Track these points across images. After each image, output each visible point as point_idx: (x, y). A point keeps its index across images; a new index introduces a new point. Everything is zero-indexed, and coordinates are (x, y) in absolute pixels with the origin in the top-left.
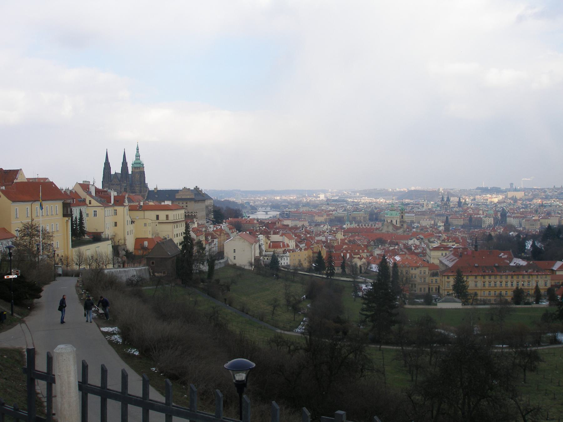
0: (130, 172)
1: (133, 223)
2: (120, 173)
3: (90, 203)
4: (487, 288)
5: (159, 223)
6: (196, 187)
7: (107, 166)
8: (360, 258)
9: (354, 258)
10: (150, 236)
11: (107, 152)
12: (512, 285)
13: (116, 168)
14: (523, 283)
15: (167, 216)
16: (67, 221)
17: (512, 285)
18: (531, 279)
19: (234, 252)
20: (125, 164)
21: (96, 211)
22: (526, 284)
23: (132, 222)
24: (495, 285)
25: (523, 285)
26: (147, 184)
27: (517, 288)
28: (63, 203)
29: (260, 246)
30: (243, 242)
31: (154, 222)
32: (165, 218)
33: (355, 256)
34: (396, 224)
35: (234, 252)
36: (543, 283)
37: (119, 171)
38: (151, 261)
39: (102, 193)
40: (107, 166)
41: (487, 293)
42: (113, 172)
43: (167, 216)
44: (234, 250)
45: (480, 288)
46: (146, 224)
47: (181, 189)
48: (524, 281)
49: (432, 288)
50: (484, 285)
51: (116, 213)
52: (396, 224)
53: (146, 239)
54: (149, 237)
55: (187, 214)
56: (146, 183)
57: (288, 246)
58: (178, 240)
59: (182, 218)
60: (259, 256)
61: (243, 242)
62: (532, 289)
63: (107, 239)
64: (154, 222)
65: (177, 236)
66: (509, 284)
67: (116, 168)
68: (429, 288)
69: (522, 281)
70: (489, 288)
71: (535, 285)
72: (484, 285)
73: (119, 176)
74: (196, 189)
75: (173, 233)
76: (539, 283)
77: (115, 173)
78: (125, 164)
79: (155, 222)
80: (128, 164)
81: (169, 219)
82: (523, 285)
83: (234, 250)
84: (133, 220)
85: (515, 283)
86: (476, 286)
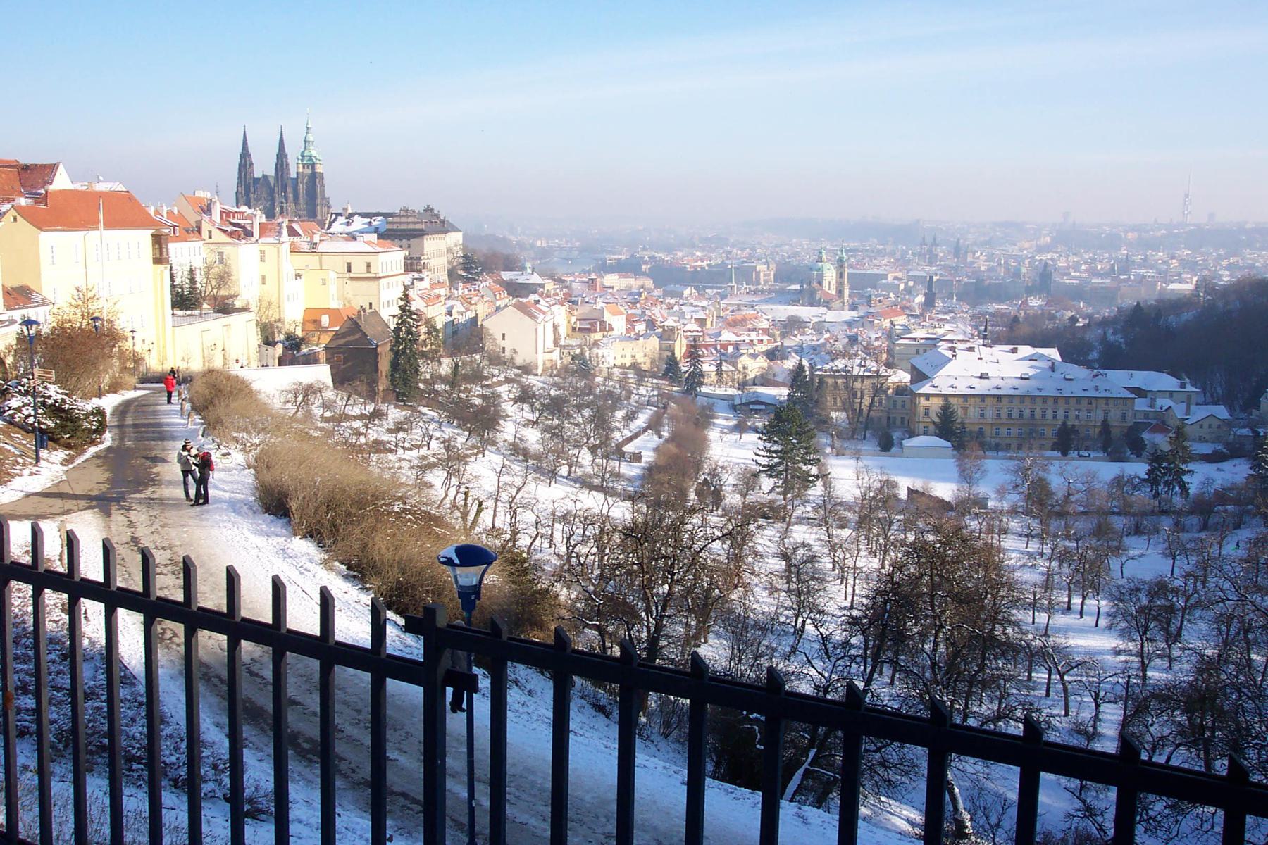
2: (273, 175)
3: (210, 237)
4: (1005, 421)
5: (352, 279)
6: (428, 206)
8: (754, 356)
9: (742, 354)
10: (334, 304)
12: (1055, 417)
13: (264, 166)
14: (1077, 413)
15: (369, 265)
16: (162, 271)
17: (1055, 417)
18: (1094, 405)
19: (504, 339)
20: (281, 155)
22: (1084, 415)
23: (298, 276)
24: (1021, 416)
25: (1077, 417)
27: (1064, 424)
28: (153, 235)
29: (555, 327)
31: (341, 276)
32: (364, 268)
36: (1119, 413)
37: (271, 172)
39: (234, 217)
41: (1003, 431)
43: (369, 265)
45: (990, 421)
48: (1079, 410)
49: (895, 418)
50: (998, 415)
53: (326, 311)
54: (331, 307)
55: (409, 261)
56: (327, 196)
57: (611, 329)
58: (389, 312)
59: (399, 267)
61: (521, 319)
62: (1095, 426)
63: (245, 309)
64: (341, 276)
65: (388, 306)
66: (1049, 415)
67: (264, 166)
68: (889, 418)
69: (1076, 410)
70: (1012, 421)
71: (1101, 418)
72: (998, 415)
73: (272, 181)
74: (428, 210)
75: (379, 298)
76: (1111, 414)
78: (281, 155)
79: (345, 276)
80: (289, 157)
82: (1077, 417)
83: (504, 335)
84: (300, 272)
85: (1061, 414)
86: (982, 415)
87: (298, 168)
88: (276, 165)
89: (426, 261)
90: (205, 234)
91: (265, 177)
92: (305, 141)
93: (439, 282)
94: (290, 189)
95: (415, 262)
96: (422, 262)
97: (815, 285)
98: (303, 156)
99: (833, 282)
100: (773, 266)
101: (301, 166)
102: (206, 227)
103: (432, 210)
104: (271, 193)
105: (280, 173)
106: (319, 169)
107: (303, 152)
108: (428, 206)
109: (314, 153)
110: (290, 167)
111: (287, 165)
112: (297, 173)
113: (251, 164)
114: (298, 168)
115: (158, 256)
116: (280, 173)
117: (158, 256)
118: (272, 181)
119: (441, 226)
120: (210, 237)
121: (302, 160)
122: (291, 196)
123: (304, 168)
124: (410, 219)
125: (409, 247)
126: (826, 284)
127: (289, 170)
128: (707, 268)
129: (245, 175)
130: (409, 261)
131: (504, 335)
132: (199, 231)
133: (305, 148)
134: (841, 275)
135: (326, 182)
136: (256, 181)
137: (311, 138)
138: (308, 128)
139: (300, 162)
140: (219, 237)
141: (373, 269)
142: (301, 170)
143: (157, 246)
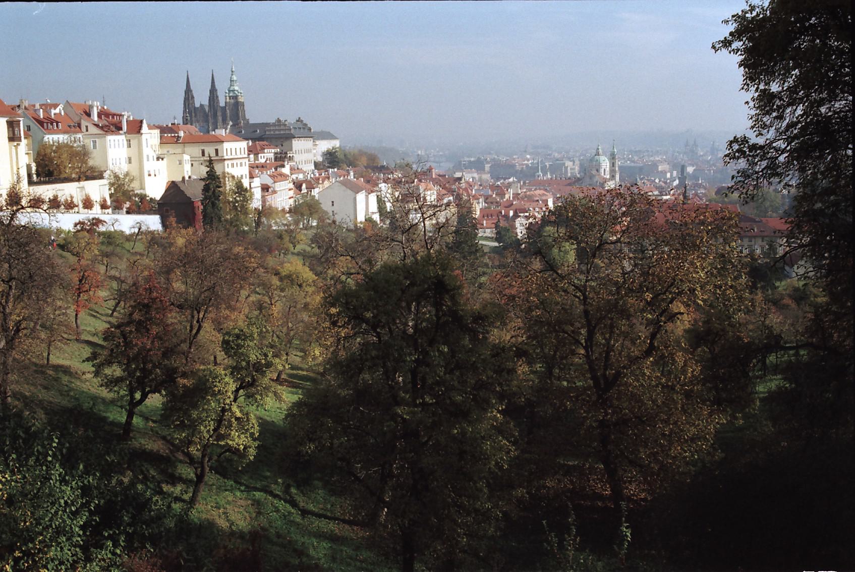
0: (222, 104)
1: (160, 160)
3: (87, 131)
6: (299, 118)
7: (188, 91)
13: (201, 98)
15: (217, 150)
18: (753, 243)
19: (333, 205)
20: (213, 91)
33: (522, 215)
34: (605, 174)
35: (333, 205)
37: (206, 102)
38: (165, 208)
40: (188, 91)
42: (197, 105)
43: (217, 150)
47: (272, 120)
48: (742, 246)
52: (605, 174)
55: (279, 156)
56: (247, 117)
67: (201, 98)
73: (207, 109)
78: (213, 91)
79: (200, 159)
81: (219, 155)
83: (333, 202)
84: (162, 156)
87: (226, 99)
88: (210, 97)
89: (291, 155)
90: (84, 129)
91: (202, 105)
92: (231, 81)
93: (298, 169)
94: (219, 114)
95: (283, 156)
96: (289, 155)
97: (594, 172)
98: (229, 91)
99: (608, 169)
100: (577, 162)
101: (228, 98)
102: (84, 124)
103: (302, 121)
104: (206, 116)
105: (212, 103)
106: (241, 99)
107: (229, 88)
108: (299, 118)
109: (236, 88)
111: (217, 97)
112: (226, 103)
113: (193, 97)
114: (226, 99)
115: (11, 136)
116: (212, 103)
117: (11, 136)
118: (207, 109)
119: (305, 131)
120: (87, 131)
121: (229, 94)
122: (220, 118)
123: (230, 99)
124: (282, 127)
125: (282, 145)
126: (602, 171)
127: (218, 100)
128: (530, 165)
129: (188, 105)
131: (333, 202)
132: (79, 126)
133: (231, 85)
134: (613, 165)
137: (235, 78)
138: (232, 71)
139: (227, 95)
140: (93, 130)
141: (220, 154)
142: (228, 100)
143: (11, 129)
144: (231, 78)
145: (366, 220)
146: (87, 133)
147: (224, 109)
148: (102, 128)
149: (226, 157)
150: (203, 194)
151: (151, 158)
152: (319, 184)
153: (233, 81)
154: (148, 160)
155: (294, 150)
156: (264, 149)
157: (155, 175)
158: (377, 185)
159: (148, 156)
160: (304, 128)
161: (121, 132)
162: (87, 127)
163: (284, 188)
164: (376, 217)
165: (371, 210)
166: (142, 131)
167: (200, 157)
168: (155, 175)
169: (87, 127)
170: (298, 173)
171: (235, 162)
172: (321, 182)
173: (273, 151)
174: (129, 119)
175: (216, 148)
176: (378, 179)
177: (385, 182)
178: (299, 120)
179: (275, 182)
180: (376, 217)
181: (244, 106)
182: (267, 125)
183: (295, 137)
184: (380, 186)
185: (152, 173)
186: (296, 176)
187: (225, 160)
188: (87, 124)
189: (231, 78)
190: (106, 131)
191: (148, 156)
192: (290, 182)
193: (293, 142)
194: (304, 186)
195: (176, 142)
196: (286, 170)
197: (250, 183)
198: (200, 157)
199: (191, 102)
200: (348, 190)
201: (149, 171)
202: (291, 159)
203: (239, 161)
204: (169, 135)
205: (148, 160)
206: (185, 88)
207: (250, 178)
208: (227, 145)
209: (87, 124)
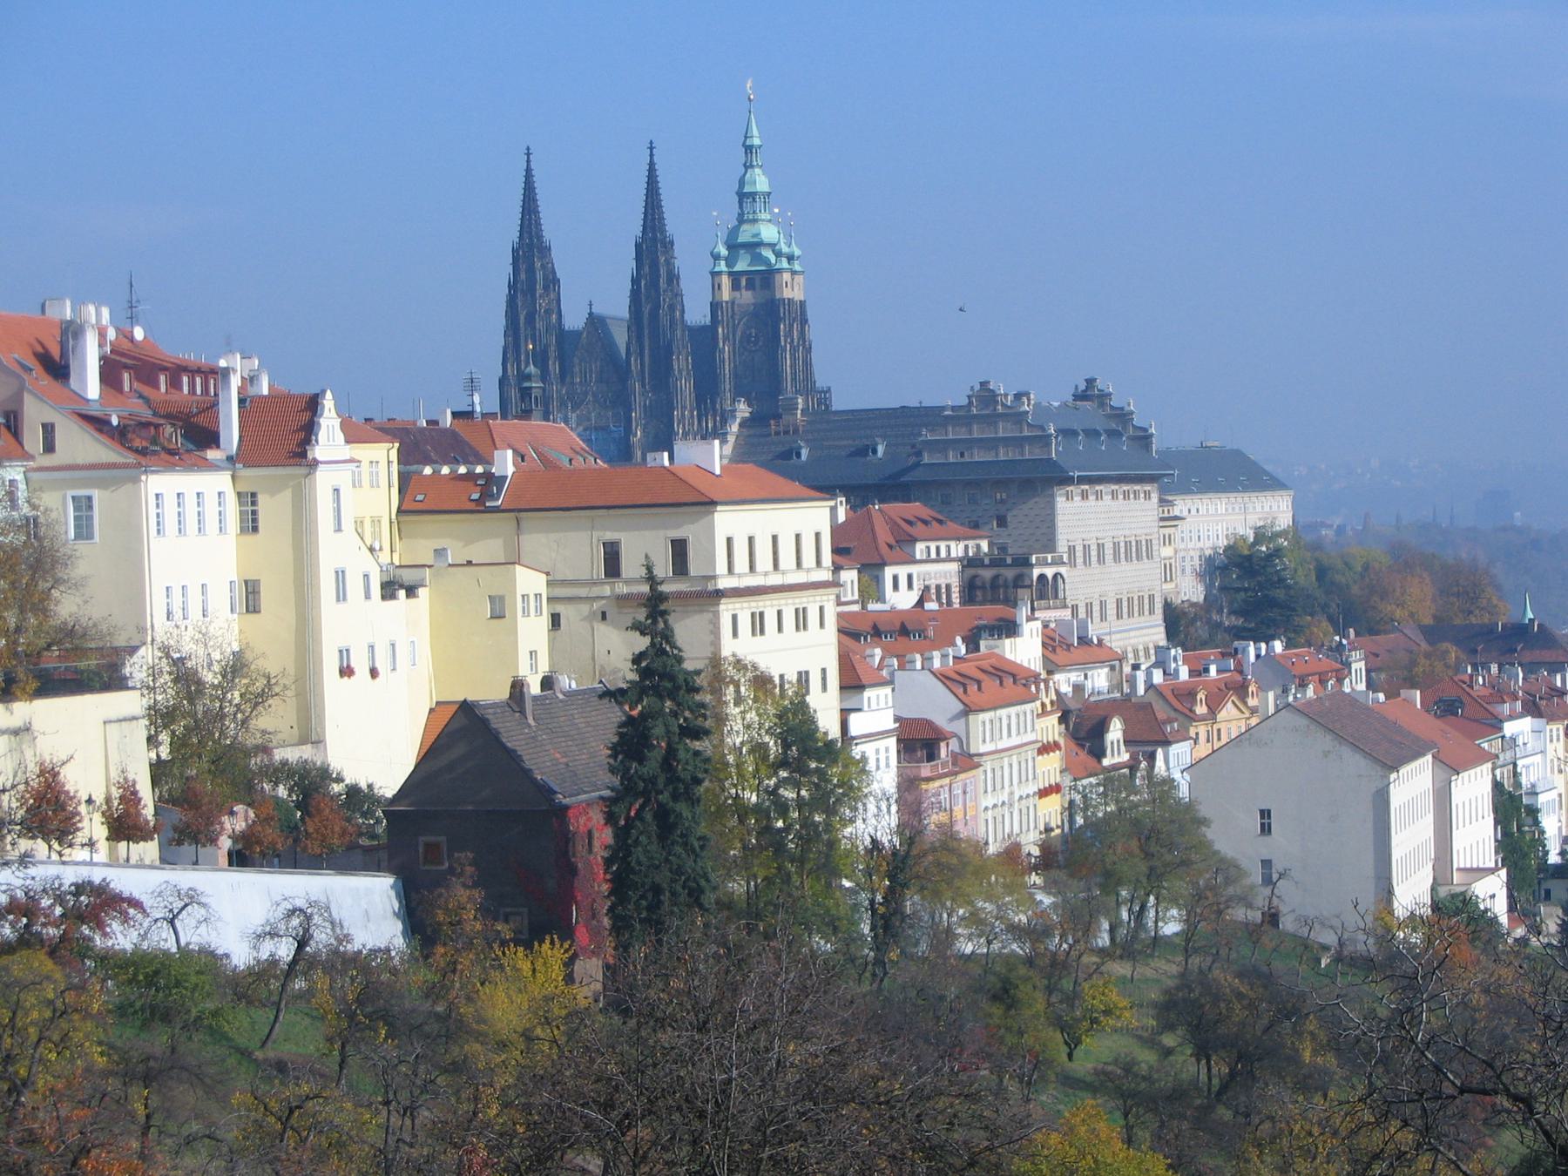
1: (402, 593)
3: (49, 447)
6: (1090, 382)
11: (528, 171)
15: (679, 549)
19: (1266, 829)
21: (89, 499)
26: (829, 390)
30: (1326, 754)
35: (1266, 829)
37: (616, 305)
38: (422, 839)
39: (175, 384)
43: (679, 549)
44: (1262, 812)
46: (502, 598)
47: (951, 394)
51: (255, 520)
55: (987, 574)
56: (821, 381)
60: (1492, 865)
61: (1326, 754)
73: (621, 337)
77: (591, 314)
79: (596, 591)
80: (678, 250)
81: (692, 572)
83: (1265, 814)
84: (408, 576)
87: (716, 287)
88: (635, 281)
89: (1049, 572)
90: (33, 439)
91: (596, 322)
93: (1084, 640)
94: (682, 363)
95: (1009, 574)
96: (1036, 572)
98: (733, 247)
101: (725, 281)
102: (35, 412)
103: (1103, 397)
104: (616, 371)
105: (646, 310)
106: (792, 289)
107: (734, 232)
108: (1090, 382)
109: (768, 232)
110: (685, 285)
111: (673, 278)
112: (715, 306)
113: (552, 282)
114: (716, 287)
116: (646, 310)
118: (621, 337)
121: (730, 261)
122: (685, 387)
123: (735, 286)
124: (1003, 429)
125: (1002, 522)
127: (678, 295)
129: (531, 319)
130: (987, 574)
131: (1265, 814)
133: (741, 220)
135: (814, 332)
136: (565, 338)
137: (760, 182)
138: (749, 149)
139: (722, 266)
140: (78, 445)
141: (694, 569)
142: (726, 294)
144: (742, 182)
145: (1436, 906)
146: (48, 461)
147: (704, 338)
148: (120, 435)
149: (724, 583)
150: (613, 770)
151: (354, 586)
152: (1192, 718)
153: (753, 195)
154: (341, 596)
155: (1062, 547)
156: (913, 540)
157: (374, 673)
158: (1495, 725)
159: (340, 576)
160: (1113, 434)
161: (212, 454)
162: (48, 430)
163: (1015, 741)
164: (1493, 893)
165: (1460, 860)
166: (319, 452)
167: (594, 583)
168: (374, 673)
169: (48, 430)
170: (1085, 665)
171: (769, 606)
172: (1201, 709)
173: (957, 549)
174: (252, 391)
175: (677, 534)
176: (1500, 693)
177: (1533, 708)
178: (1088, 393)
179: (968, 711)
180: (1493, 893)
181: (804, 322)
182: (930, 416)
183: (1068, 481)
184: (1510, 728)
185: (360, 665)
186: (1075, 677)
187: (719, 594)
188: (50, 415)
189: (742, 182)
190: (142, 452)
191: (340, 576)
192: (1044, 712)
193: (1061, 502)
194: (1115, 732)
195: (480, 507)
196: (1025, 649)
197: (845, 713)
198: (594, 583)
199: (541, 304)
200: (1346, 752)
201: (344, 653)
202: (1047, 590)
203: (788, 603)
204: (445, 470)
205: (341, 596)
206: (513, 234)
207: (843, 688)
208: (730, 522)
209: (50, 415)
